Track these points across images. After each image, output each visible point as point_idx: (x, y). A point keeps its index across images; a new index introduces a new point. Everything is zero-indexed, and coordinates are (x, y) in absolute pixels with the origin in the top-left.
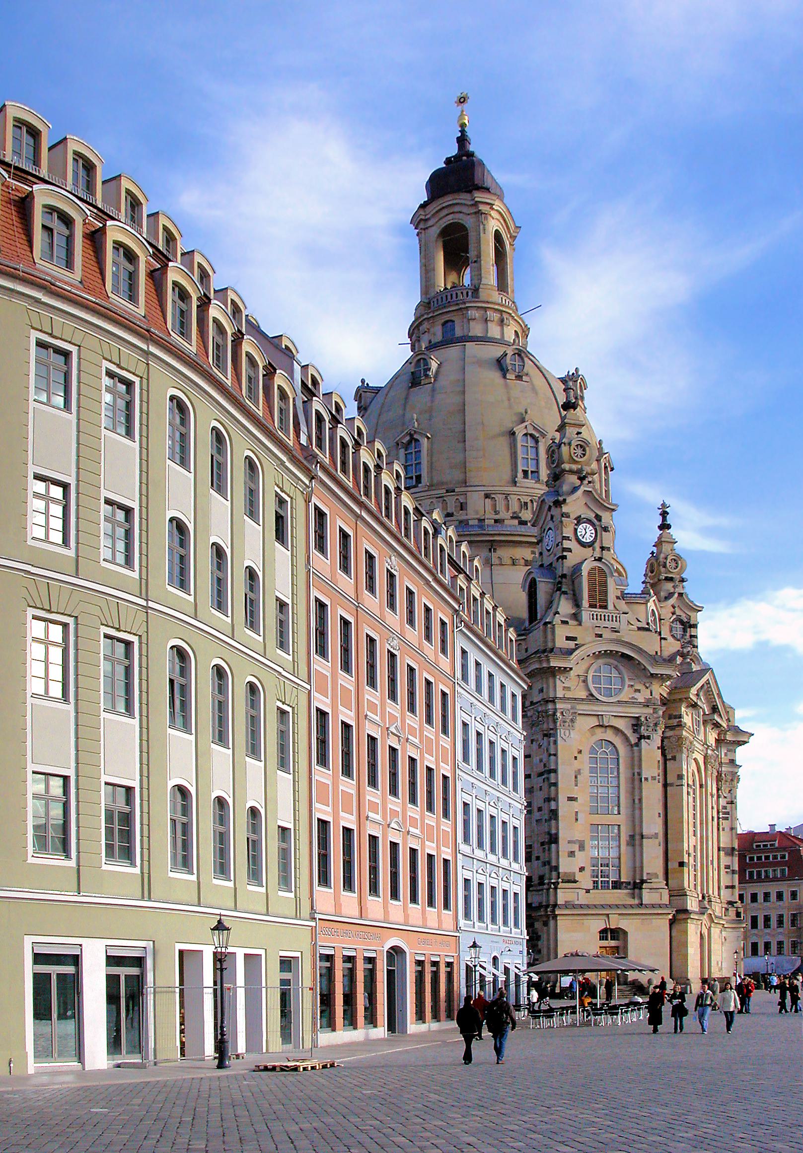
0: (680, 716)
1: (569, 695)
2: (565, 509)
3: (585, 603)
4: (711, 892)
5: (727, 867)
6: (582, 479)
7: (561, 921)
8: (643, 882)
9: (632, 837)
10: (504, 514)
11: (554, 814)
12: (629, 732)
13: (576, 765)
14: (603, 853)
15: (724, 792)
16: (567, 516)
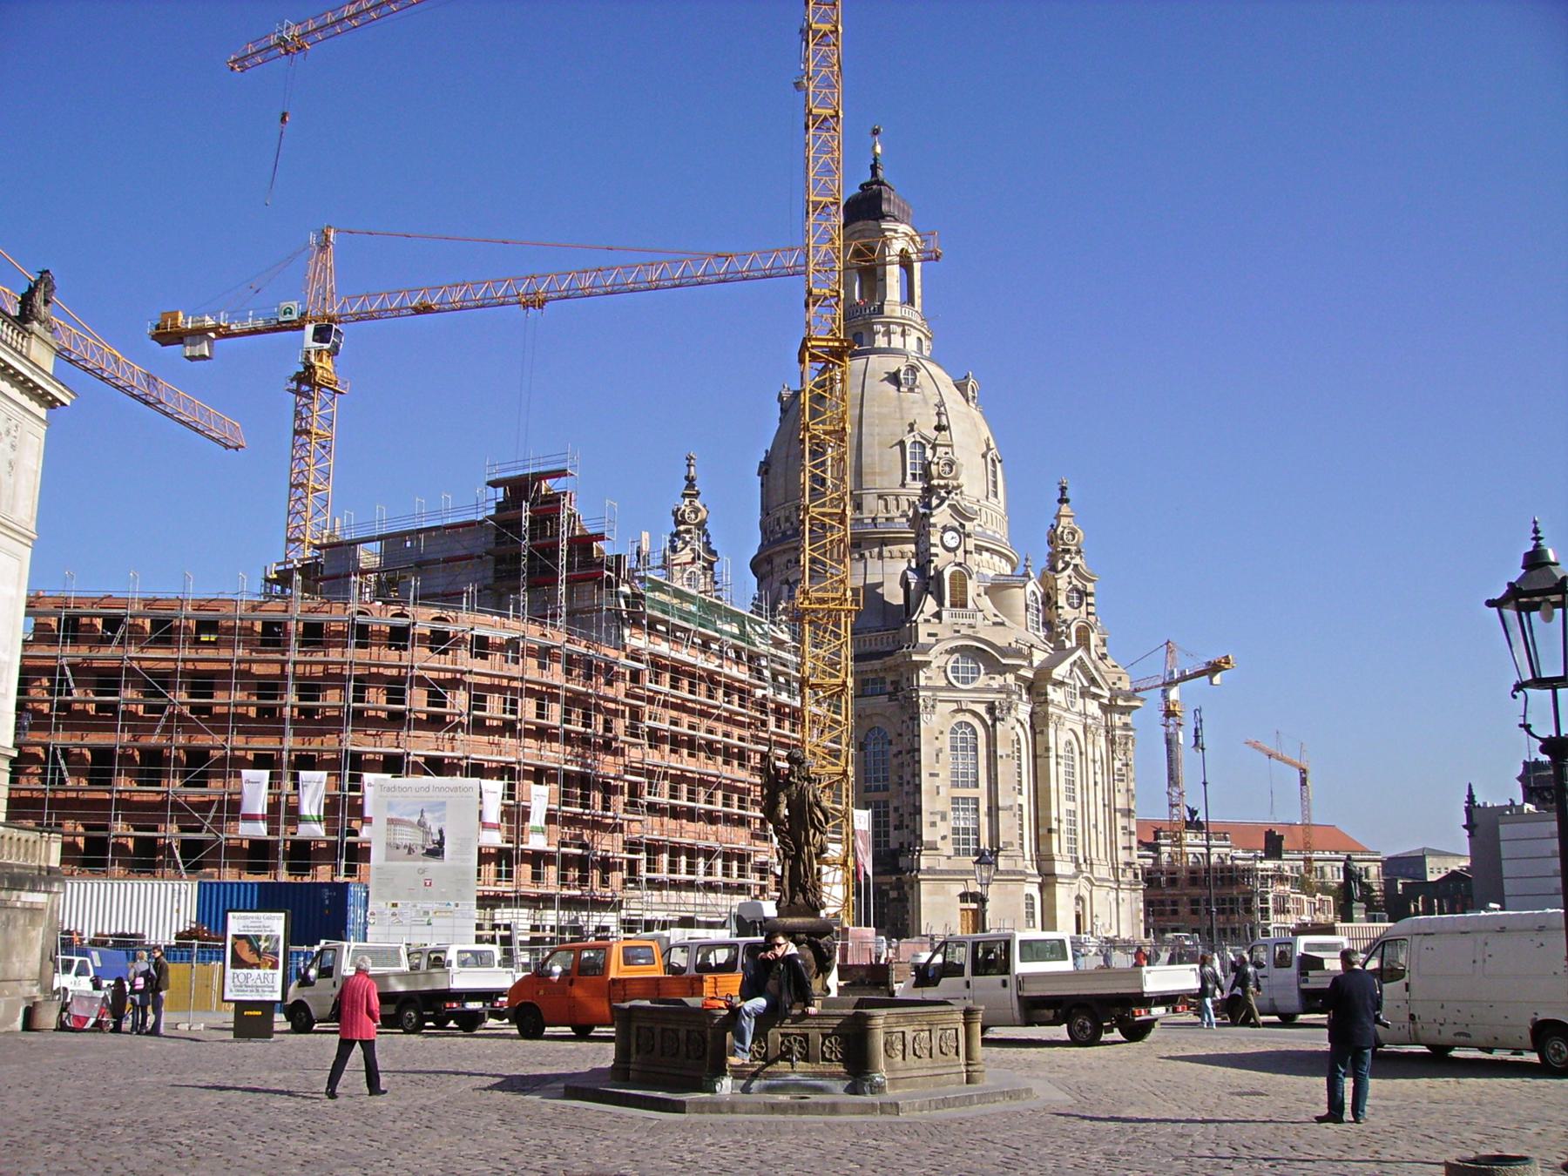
0: (1046, 694)
1: (930, 683)
2: (932, 520)
3: (947, 603)
4: (1094, 855)
5: (1124, 828)
6: (948, 493)
7: (923, 886)
8: (999, 849)
9: (990, 808)
10: (894, 513)
11: (919, 786)
12: (987, 717)
13: (938, 744)
14: (962, 825)
15: (1119, 754)
16: (935, 525)
